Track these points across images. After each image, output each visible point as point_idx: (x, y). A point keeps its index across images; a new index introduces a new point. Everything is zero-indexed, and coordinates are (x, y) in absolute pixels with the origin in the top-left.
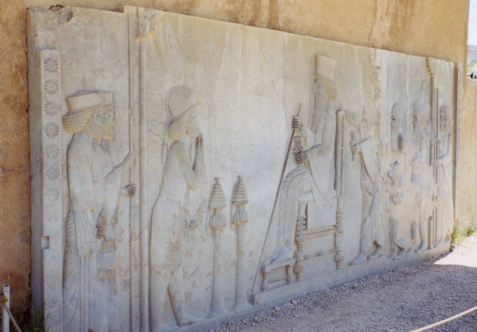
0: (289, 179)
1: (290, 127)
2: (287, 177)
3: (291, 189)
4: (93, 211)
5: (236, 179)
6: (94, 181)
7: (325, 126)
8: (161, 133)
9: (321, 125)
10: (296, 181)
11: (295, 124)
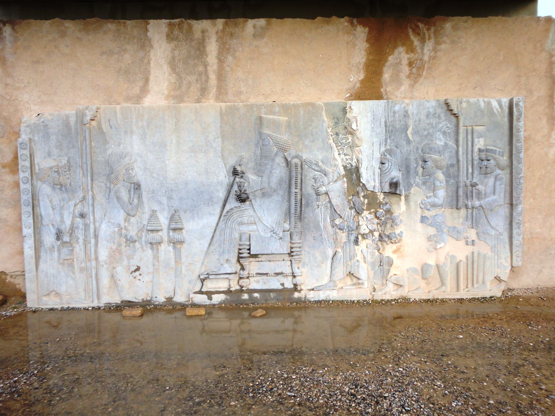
0: (229, 213)
1: (231, 174)
2: (228, 212)
3: (230, 221)
4: (53, 225)
5: (172, 211)
6: (53, 209)
7: (271, 172)
8: (105, 181)
9: (267, 172)
10: (236, 215)
11: (235, 173)
